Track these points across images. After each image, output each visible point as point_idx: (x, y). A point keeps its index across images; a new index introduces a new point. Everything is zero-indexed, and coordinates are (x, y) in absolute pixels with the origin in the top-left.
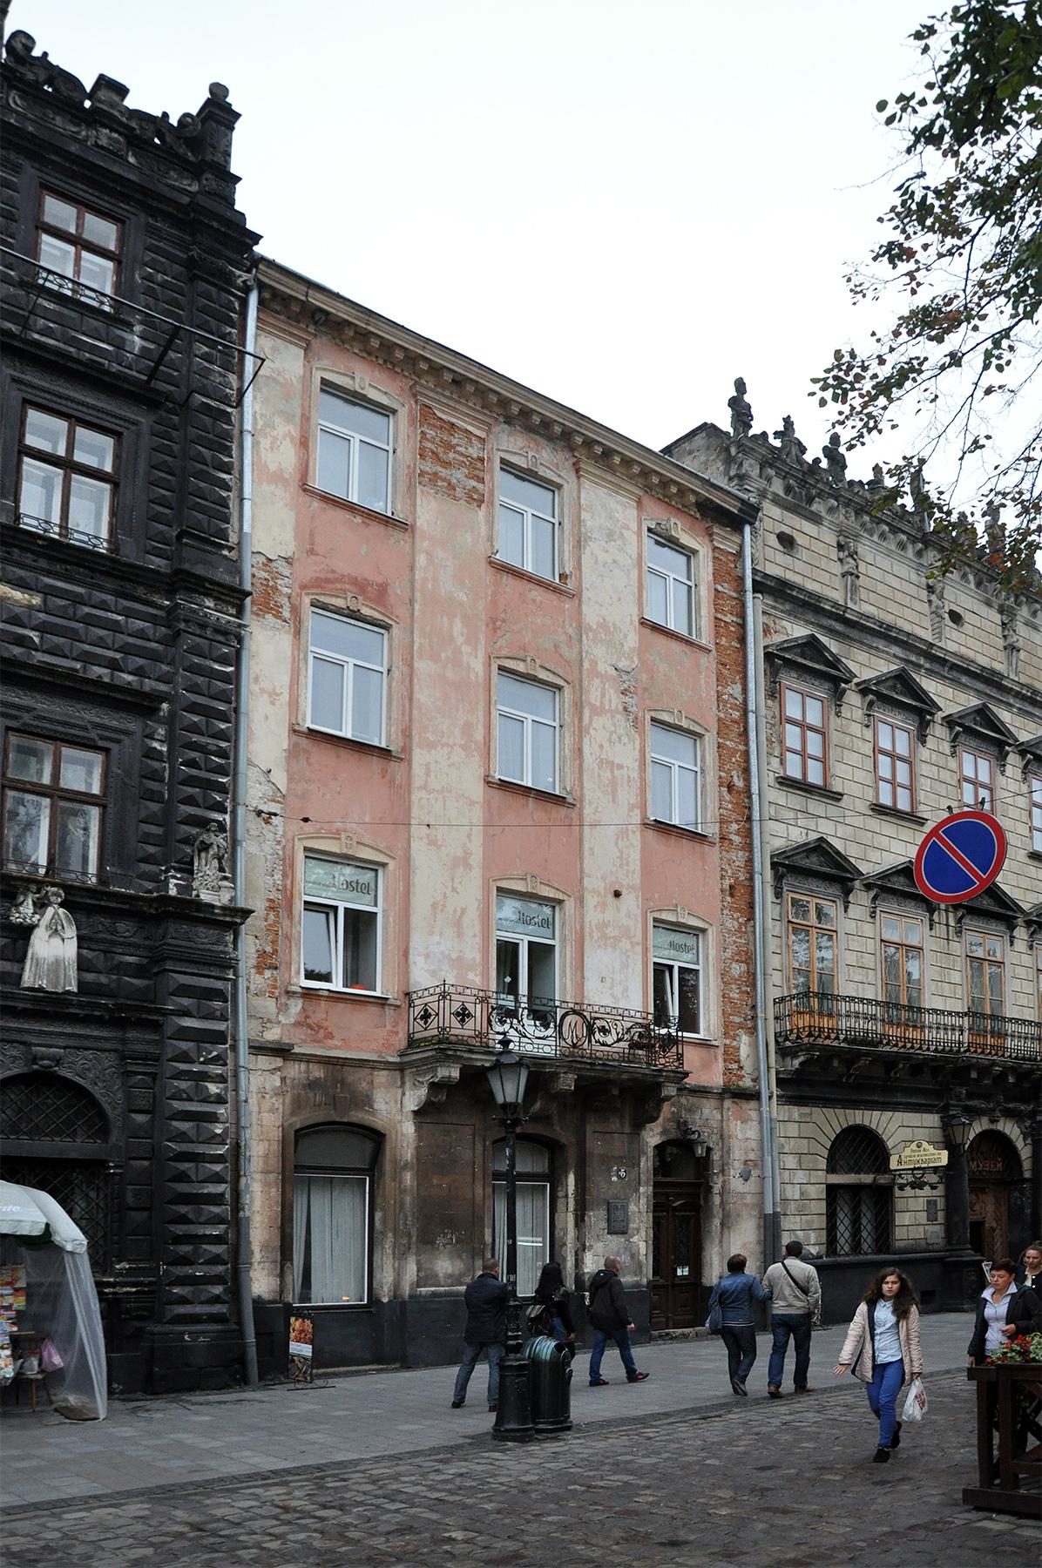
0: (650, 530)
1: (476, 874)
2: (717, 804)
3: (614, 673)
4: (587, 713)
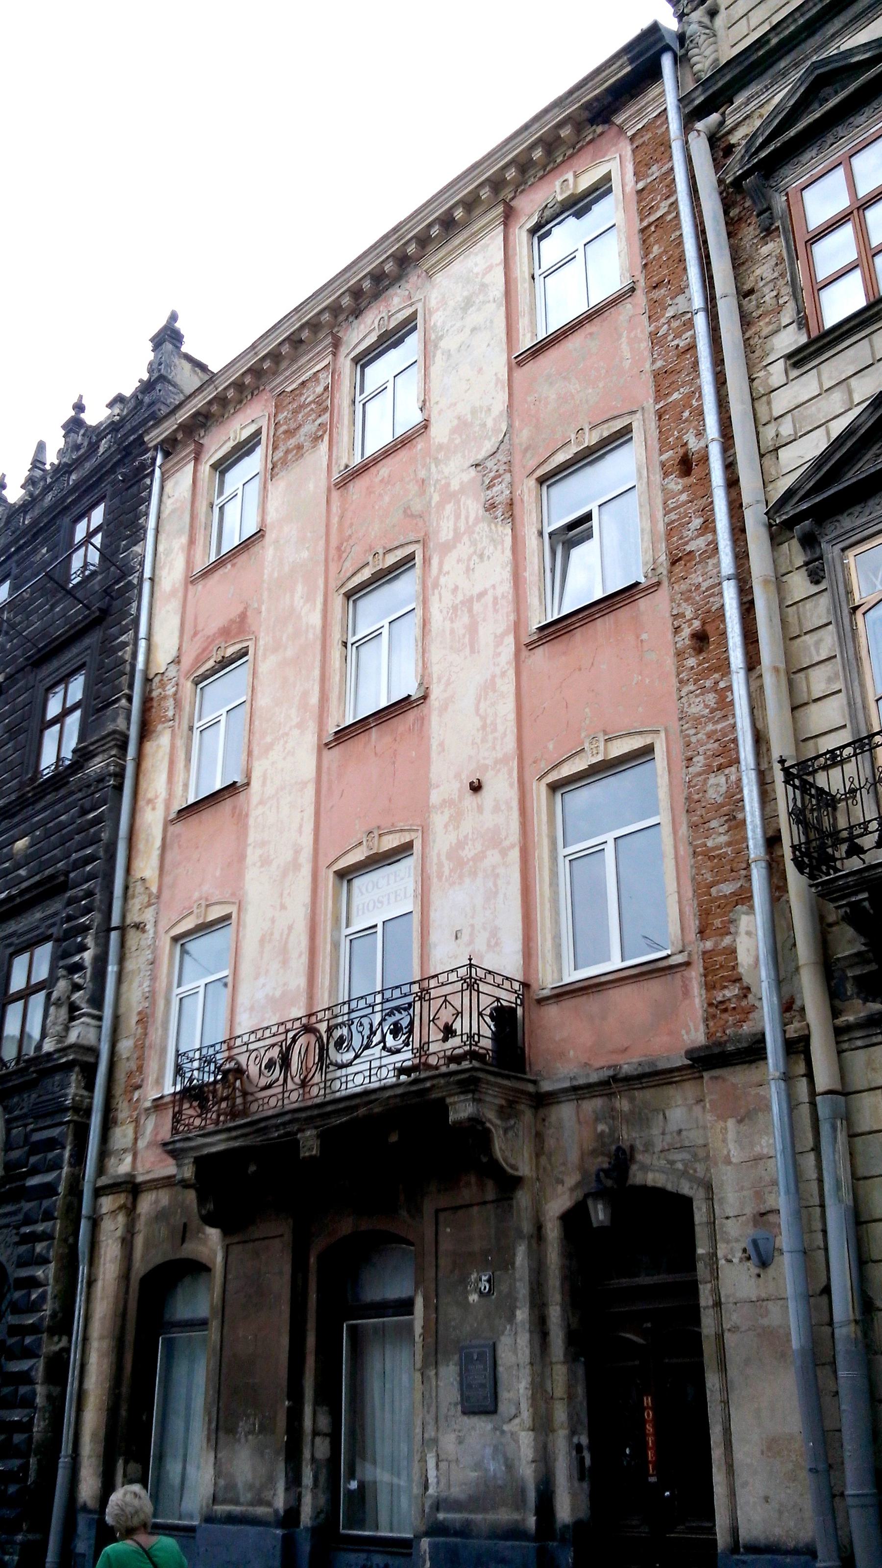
0: (533, 231)
1: (306, 871)
2: (660, 513)
3: (473, 472)
4: (435, 562)
